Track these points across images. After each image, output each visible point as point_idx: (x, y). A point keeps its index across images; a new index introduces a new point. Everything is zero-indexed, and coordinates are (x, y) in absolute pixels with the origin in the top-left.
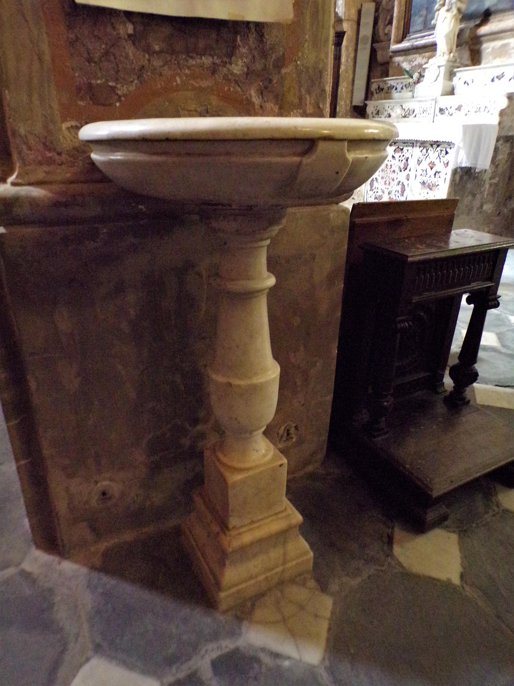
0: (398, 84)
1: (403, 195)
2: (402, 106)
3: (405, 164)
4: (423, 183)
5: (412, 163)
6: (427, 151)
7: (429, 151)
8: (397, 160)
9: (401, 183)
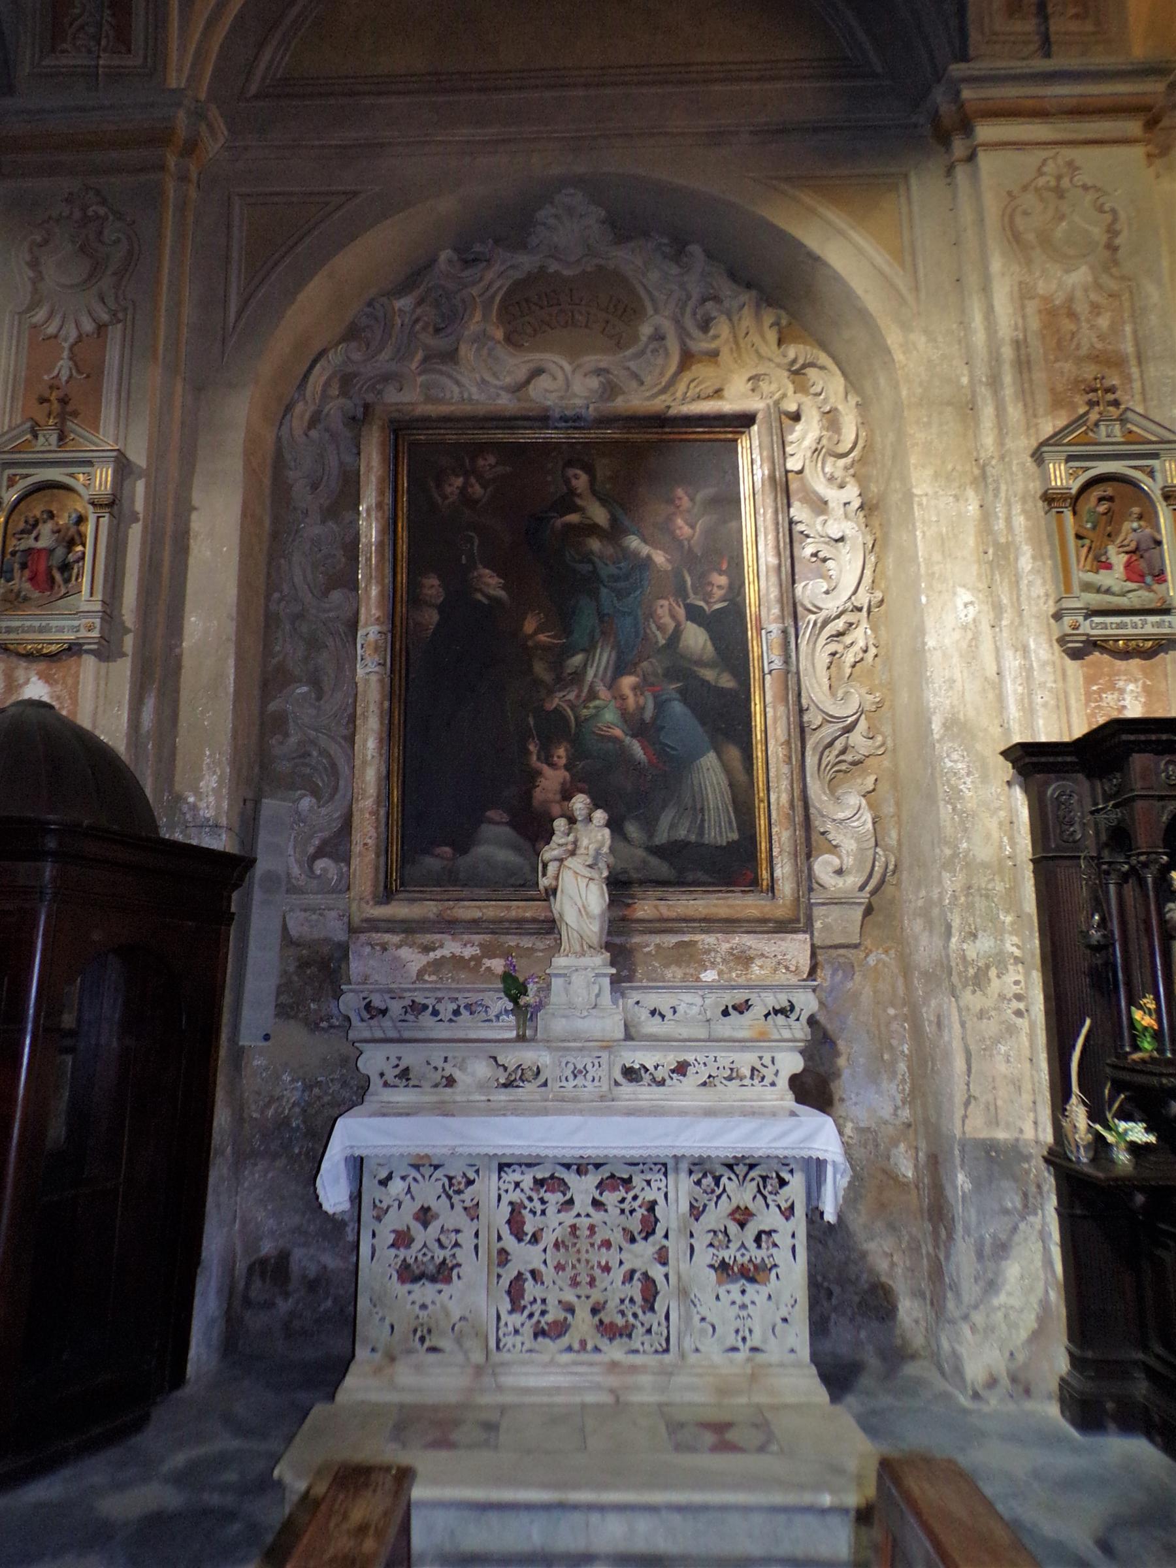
0: (439, 1000)
1: (652, 1309)
2: (495, 1059)
3: (644, 1220)
4: (723, 1268)
5: (671, 1215)
6: (717, 1180)
7: (724, 1180)
8: (614, 1211)
9: (637, 1275)
